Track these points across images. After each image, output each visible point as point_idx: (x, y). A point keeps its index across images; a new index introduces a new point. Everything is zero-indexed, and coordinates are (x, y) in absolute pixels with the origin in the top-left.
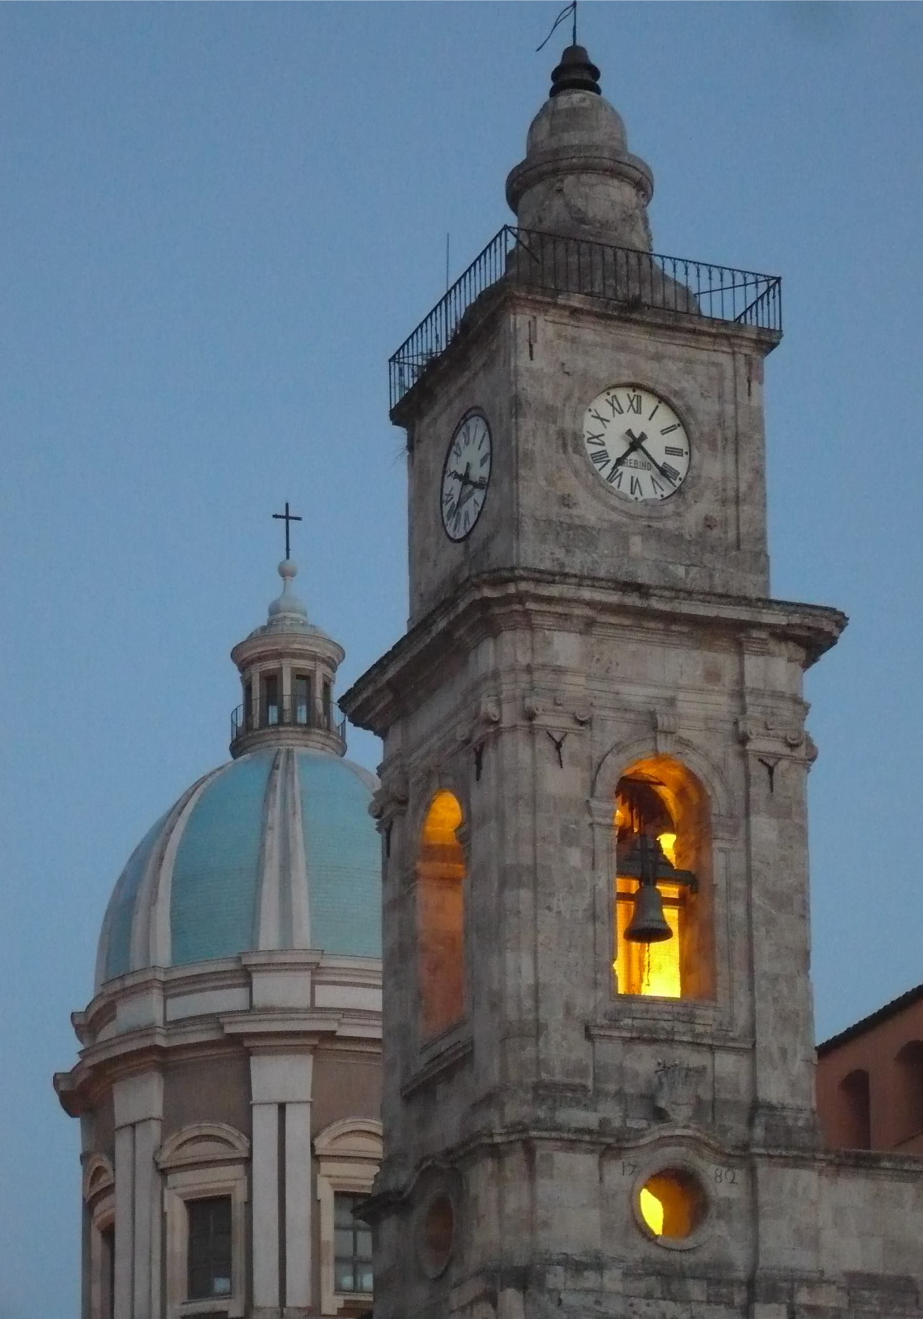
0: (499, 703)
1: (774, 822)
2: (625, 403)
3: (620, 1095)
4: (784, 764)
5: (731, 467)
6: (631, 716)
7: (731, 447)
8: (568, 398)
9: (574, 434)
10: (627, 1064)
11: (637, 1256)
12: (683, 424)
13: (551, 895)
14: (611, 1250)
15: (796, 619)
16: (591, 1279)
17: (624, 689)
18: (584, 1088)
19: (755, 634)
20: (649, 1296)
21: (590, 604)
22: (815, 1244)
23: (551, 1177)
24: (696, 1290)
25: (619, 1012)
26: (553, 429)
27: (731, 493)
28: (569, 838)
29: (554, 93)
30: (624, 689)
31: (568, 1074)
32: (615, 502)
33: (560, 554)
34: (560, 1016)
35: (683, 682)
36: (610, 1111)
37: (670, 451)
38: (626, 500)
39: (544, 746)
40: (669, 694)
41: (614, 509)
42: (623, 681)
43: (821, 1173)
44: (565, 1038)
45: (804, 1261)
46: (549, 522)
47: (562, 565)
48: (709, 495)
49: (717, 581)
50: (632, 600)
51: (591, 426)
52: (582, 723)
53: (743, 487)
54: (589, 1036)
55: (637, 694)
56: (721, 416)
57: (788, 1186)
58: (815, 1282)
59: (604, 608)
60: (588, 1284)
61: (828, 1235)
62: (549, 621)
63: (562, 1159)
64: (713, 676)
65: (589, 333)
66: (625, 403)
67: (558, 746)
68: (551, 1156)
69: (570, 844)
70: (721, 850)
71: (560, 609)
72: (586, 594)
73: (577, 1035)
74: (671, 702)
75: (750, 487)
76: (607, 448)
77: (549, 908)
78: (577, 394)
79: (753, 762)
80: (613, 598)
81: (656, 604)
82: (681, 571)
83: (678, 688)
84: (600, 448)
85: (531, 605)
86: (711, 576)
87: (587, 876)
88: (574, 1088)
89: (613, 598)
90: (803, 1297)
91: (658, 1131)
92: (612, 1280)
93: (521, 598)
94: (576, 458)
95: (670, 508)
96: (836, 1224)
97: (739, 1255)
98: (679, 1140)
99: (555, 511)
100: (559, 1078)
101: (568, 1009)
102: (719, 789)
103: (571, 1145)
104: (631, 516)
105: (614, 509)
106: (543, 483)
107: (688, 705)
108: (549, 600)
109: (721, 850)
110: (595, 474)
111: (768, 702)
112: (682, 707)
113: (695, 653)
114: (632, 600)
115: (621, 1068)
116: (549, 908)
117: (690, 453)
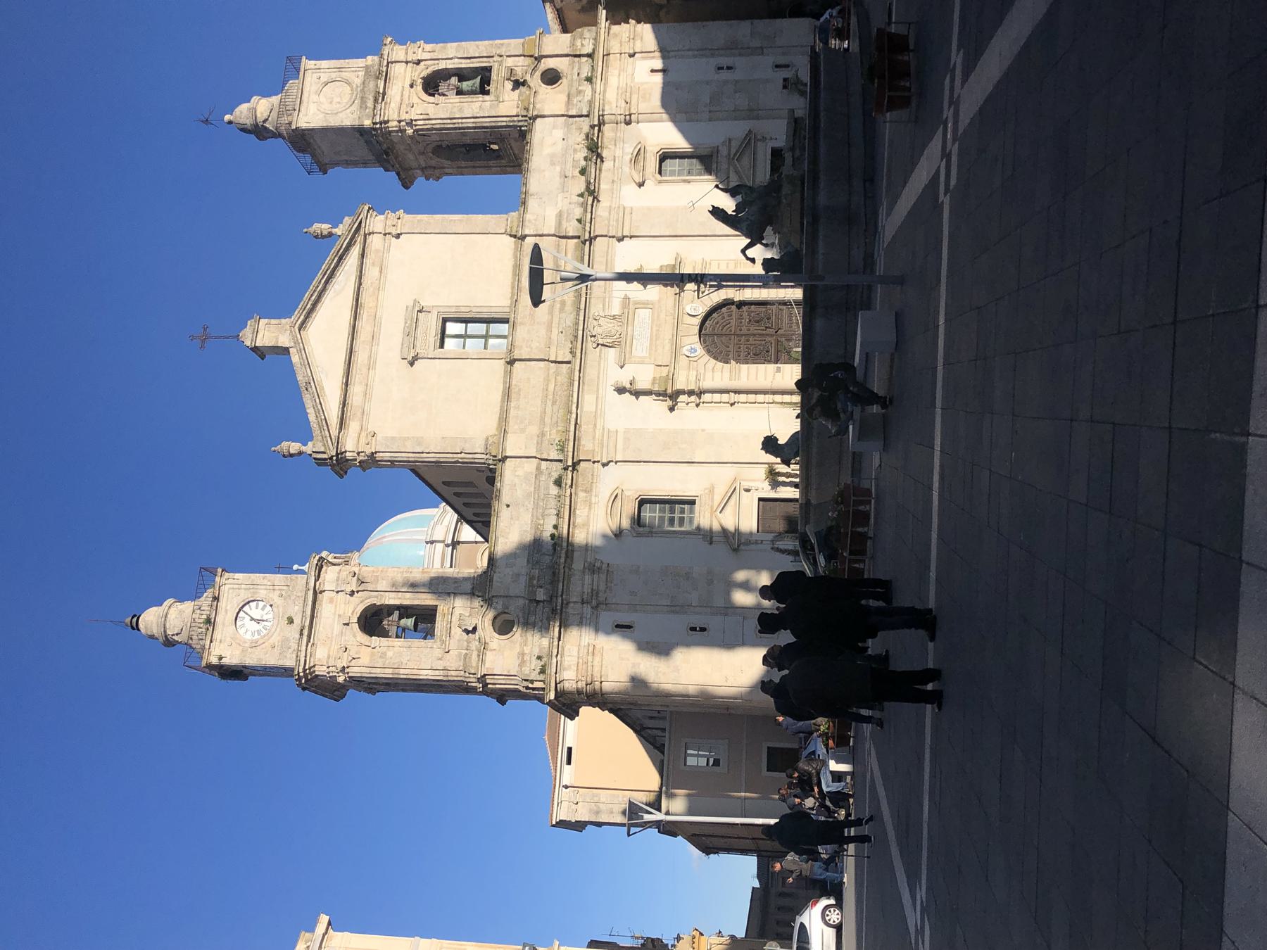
0: (339, 676)
1: (380, 582)
2: (241, 623)
3: (468, 642)
5: (262, 587)
6: (344, 631)
7: (255, 586)
8: (240, 645)
9: (251, 643)
10: (458, 638)
11: (520, 638)
12: (248, 602)
13: (402, 663)
14: (517, 649)
16: (527, 658)
17: (335, 633)
18: (466, 654)
21: (307, 646)
22: (518, 575)
23: (493, 669)
25: (440, 640)
26: (250, 650)
27: (271, 587)
28: (383, 655)
30: (335, 633)
31: (460, 660)
32: (273, 630)
33: (290, 651)
34: (441, 662)
35: (333, 611)
36: (474, 645)
37: (257, 608)
38: (273, 625)
39: (353, 663)
40: (337, 616)
41: (276, 630)
43: (495, 572)
44: (449, 660)
45: (523, 579)
46: (280, 654)
47: (294, 650)
48: (271, 595)
49: (299, 594)
50: (306, 632)
51: (248, 637)
52: (346, 649)
53: (269, 583)
54: (448, 652)
55: (338, 627)
56: (245, 589)
57: (499, 584)
58: (531, 579)
59: (309, 641)
60: (529, 659)
62: (312, 660)
63: (487, 665)
64: (331, 601)
65: (217, 636)
66: (241, 623)
67: (354, 659)
68: (487, 668)
69: (386, 655)
70: (388, 601)
72: (304, 648)
74: (339, 616)
75: (269, 581)
76: (256, 630)
77: (407, 664)
78: (238, 642)
79: (359, 589)
82: (297, 608)
83: (335, 614)
84: (256, 633)
85: (307, 667)
86: (298, 597)
87: (396, 649)
88: (465, 658)
89: (305, 638)
90: (535, 582)
91: (479, 627)
92: (527, 650)
93: (305, 670)
94: (259, 643)
95: (275, 609)
96: (512, 567)
97: (521, 602)
99: (277, 651)
100: (462, 664)
101: (440, 659)
102: (368, 601)
104: (278, 624)
105: (276, 630)
106: (267, 655)
108: (305, 664)
109: (388, 601)
110: (264, 636)
111: (340, 582)
112: (341, 613)
113: (324, 606)
114: (306, 632)
115: (459, 641)
116: (407, 664)
117: (258, 600)
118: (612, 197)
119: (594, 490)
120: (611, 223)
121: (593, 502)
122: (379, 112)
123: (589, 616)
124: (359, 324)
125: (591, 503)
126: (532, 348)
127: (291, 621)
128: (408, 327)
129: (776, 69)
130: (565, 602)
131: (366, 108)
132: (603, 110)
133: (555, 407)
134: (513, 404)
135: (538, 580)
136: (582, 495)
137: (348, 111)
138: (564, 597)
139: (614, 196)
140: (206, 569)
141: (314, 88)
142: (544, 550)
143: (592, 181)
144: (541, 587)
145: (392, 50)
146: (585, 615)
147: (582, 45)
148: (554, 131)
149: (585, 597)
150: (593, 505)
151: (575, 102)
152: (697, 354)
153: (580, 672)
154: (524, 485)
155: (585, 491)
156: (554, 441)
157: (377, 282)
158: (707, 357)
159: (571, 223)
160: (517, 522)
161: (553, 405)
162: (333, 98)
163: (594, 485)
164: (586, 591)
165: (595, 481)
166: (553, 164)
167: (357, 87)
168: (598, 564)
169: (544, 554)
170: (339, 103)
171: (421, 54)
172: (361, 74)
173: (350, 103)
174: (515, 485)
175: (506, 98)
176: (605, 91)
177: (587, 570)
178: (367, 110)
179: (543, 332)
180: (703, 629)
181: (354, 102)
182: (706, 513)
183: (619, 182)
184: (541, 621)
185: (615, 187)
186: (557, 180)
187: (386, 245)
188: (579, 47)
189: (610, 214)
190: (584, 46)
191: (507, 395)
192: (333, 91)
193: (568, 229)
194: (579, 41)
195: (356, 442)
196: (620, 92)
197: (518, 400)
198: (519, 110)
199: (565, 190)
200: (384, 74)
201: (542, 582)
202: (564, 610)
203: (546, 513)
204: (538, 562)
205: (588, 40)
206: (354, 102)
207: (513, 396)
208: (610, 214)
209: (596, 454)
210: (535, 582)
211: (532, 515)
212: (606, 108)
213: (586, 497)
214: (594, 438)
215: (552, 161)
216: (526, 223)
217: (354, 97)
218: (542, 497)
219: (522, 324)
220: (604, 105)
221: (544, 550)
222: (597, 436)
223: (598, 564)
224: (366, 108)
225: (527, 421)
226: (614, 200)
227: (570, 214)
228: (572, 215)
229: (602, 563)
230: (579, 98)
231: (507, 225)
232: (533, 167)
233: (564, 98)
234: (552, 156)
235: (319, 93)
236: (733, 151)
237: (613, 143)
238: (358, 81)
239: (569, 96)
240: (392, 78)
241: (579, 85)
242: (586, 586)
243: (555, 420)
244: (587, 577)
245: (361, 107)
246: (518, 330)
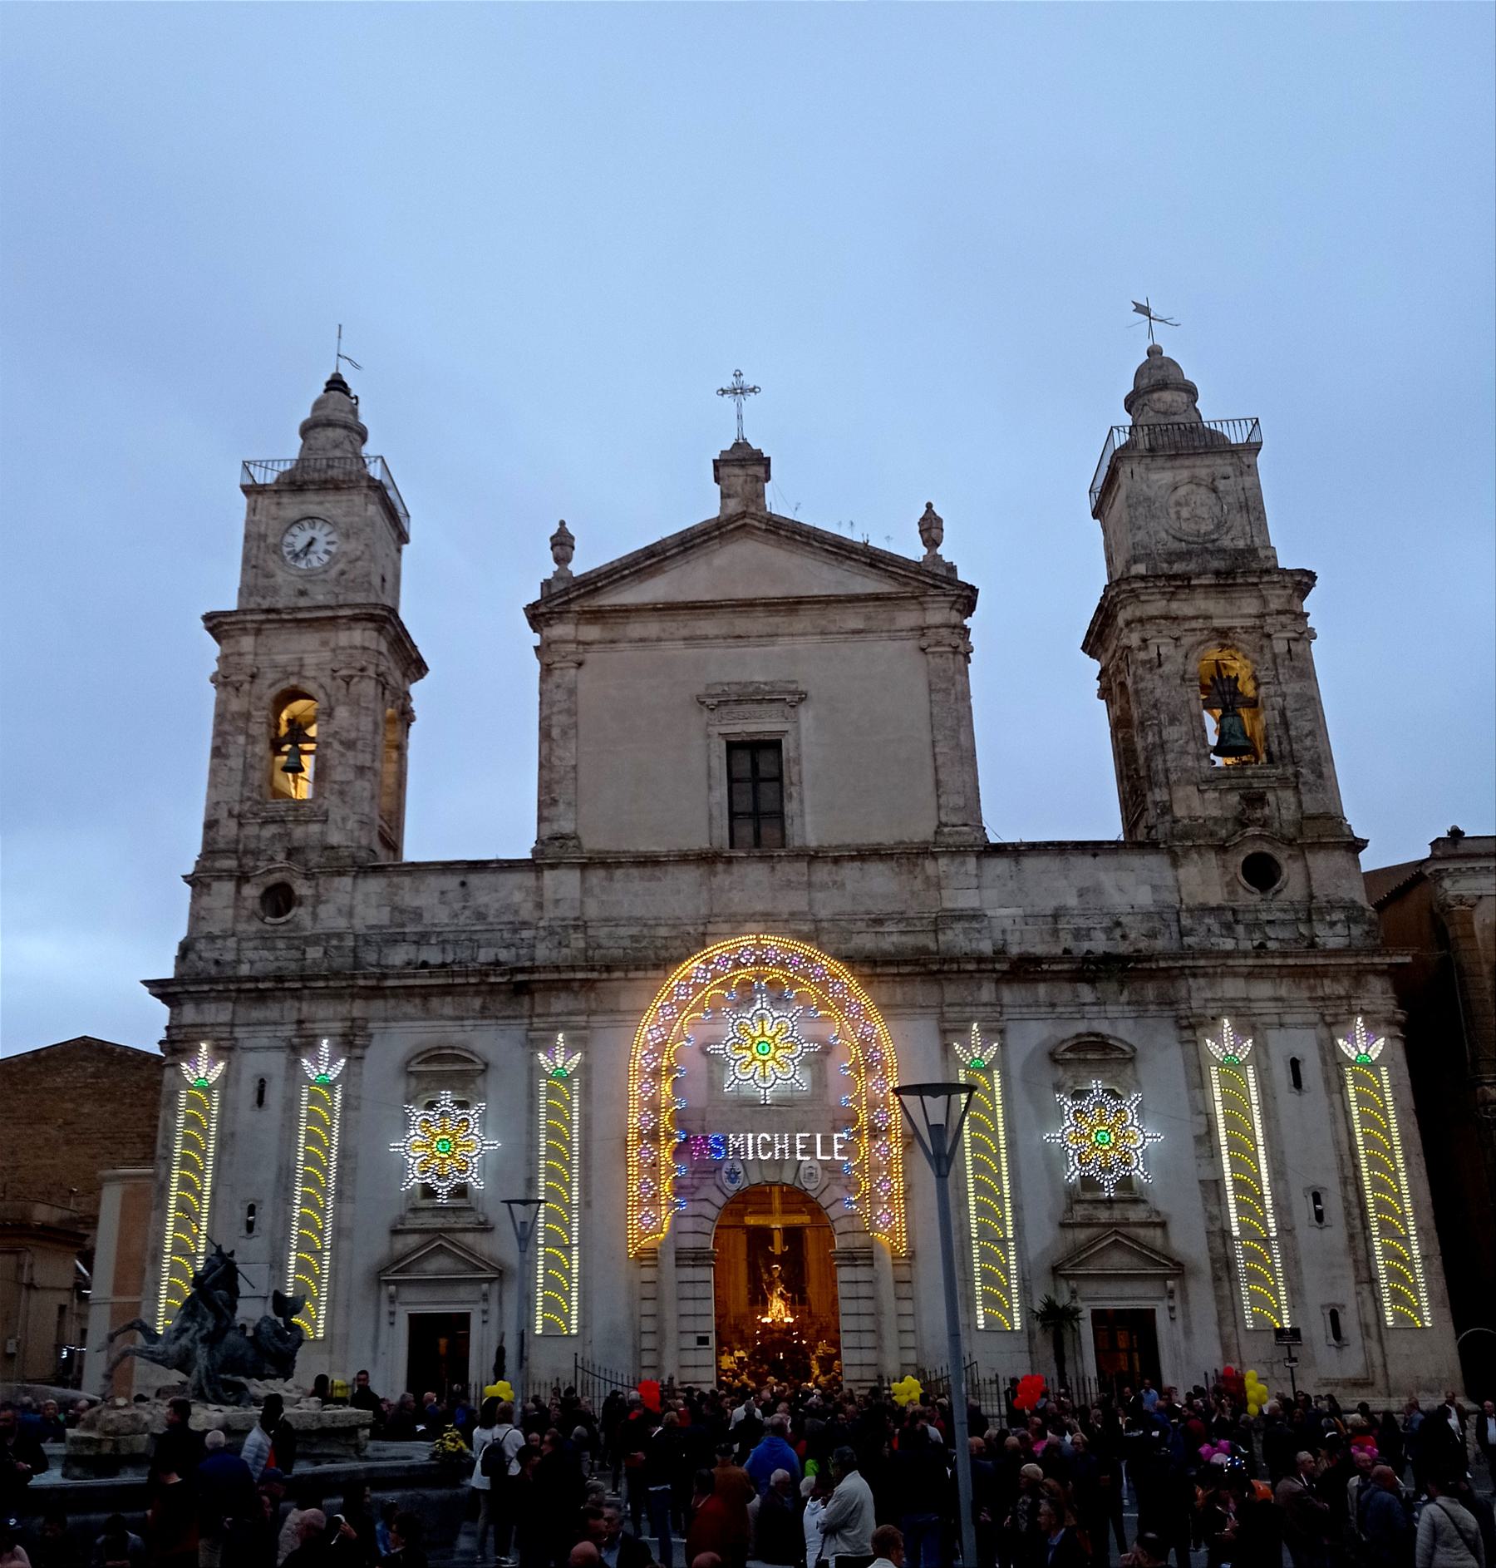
4: (356, 680)
15: (357, 611)
16: (219, 943)
19: (340, 621)
20: (256, 949)
21: (253, 621)
22: (350, 914)
24: (281, 944)
29: (326, 391)
34: (225, 814)
42: (279, 653)
45: (341, 924)
58: (340, 936)
59: (262, 622)
61: (360, 909)
64: (324, 643)
71: (240, 626)
73: (233, 824)
80: (262, 617)
81: (285, 616)
85: (226, 627)
89: (262, 617)
98: (281, 870)
103: (219, 878)
107: (310, 660)
115: (258, 837)
118: (1020, 1006)
119: (485, 1022)
120: (968, 1009)
121: (466, 1022)
122: (1151, 585)
123: (279, 1034)
124: (760, 612)
125: (462, 1019)
126: (731, 890)
127: (302, 593)
128: (759, 688)
129: (1327, 1311)
130: (299, 993)
131: (1170, 563)
132: (1194, 976)
133: (627, 943)
134: (634, 872)
135: (336, 947)
136: (477, 1003)
137: (1163, 535)
138: (306, 992)
139: (1025, 1010)
140: (383, 461)
141: (1203, 473)
142: (385, 950)
143: (1045, 967)
144: (325, 953)
145: (1285, 587)
146: (280, 1028)
147: (1333, 924)
148: (1149, 887)
149: (308, 1025)
150: (459, 1023)
151: (1207, 921)
152: (728, 1184)
153: (190, 1030)
154: (497, 905)
155: (484, 1008)
156: (567, 946)
157: (834, 629)
158: (720, 1200)
159: (961, 936)
160: (436, 901)
161: (632, 937)
162: (1187, 504)
163: (493, 1022)
164: (317, 1025)
165: (500, 1022)
166: (1081, 893)
167: (1214, 541)
168: (358, 1041)
169: (380, 951)
170: (1179, 518)
171: (1283, 639)
172: (1241, 544)
173: (1178, 535)
174: (496, 891)
175: (1211, 795)
176: (1235, 975)
177: (349, 1024)
178: (1165, 565)
179: (759, 907)
180: (250, 1227)
181: (1181, 540)
182: (443, 1220)
183: (1054, 1016)
184: (277, 959)
185: (1043, 1009)
186: (1048, 905)
187: (904, 633)
188: (1328, 918)
189: (985, 1005)
190: (1331, 928)
191: (648, 862)
192: (1202, 505)
193: (949, 932)
194: (1343, 918)
195: (566, 638)
196: (1239, 1004)
197: (642, 879)
198: (1186, 821)
199: (1030, 920)
200: (1230, 581)
201: (333, 952)
202: (287, 993)
203: (448, 947)
204: (367, 943)
205: (1347, 933)
206: (1181, 540)
207: (648, 871)
208: (985, 1005)
209: (544, 1019)
210: (334, 942)
211: (447, 925)
212: (1202, 981)
213: (474, 1010)
214: (570, 1014)
215: (1088, 889)
216: (958, 860)
217: (1191, 539)
218: (475, 937)
219: (773, 869)
220: (1205, 975)
221: (385, 950)
222: (573, 1018)
223: (358, 1041)
224: (1170, 563)
225: (604, 897)
226: (1018, 1010)
227: (979, 932)
228: (977, 935)
229: (365, 1047)
230: (1216, 928)
231: (954, 826)
232: (1072, 859)
233: (1216, 897)
234: (1098, 890)
235: (1194, 481)
236: (1123, 1230)
237: (1134, 998)
238: (1226, 542)
239: (1218, 910)
240: (1227, 595)
241: (1247, 926)
242: (323, 1025)
243: (605, 942)
244: (339, 1024)
245: (1170, 554)
246: (760, 866)
